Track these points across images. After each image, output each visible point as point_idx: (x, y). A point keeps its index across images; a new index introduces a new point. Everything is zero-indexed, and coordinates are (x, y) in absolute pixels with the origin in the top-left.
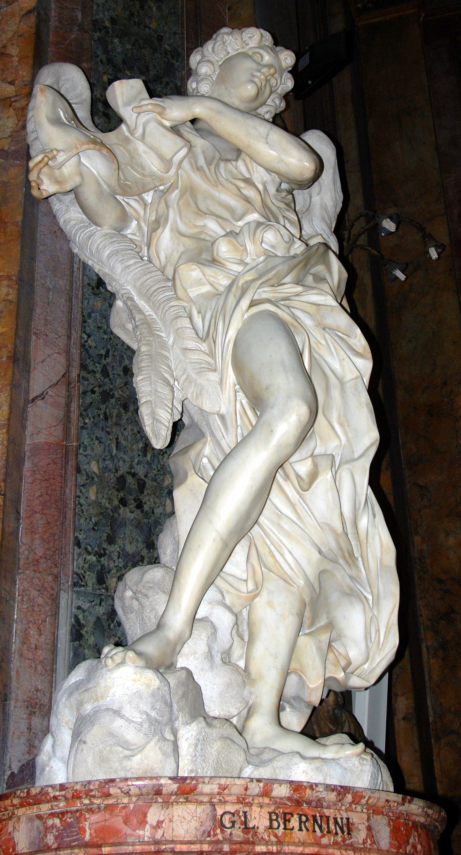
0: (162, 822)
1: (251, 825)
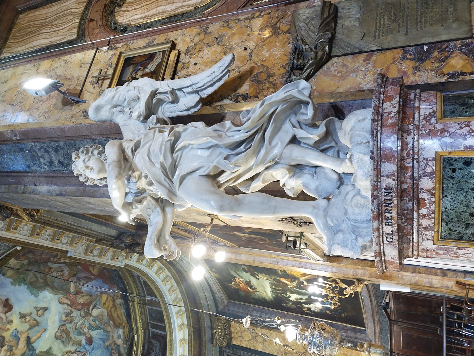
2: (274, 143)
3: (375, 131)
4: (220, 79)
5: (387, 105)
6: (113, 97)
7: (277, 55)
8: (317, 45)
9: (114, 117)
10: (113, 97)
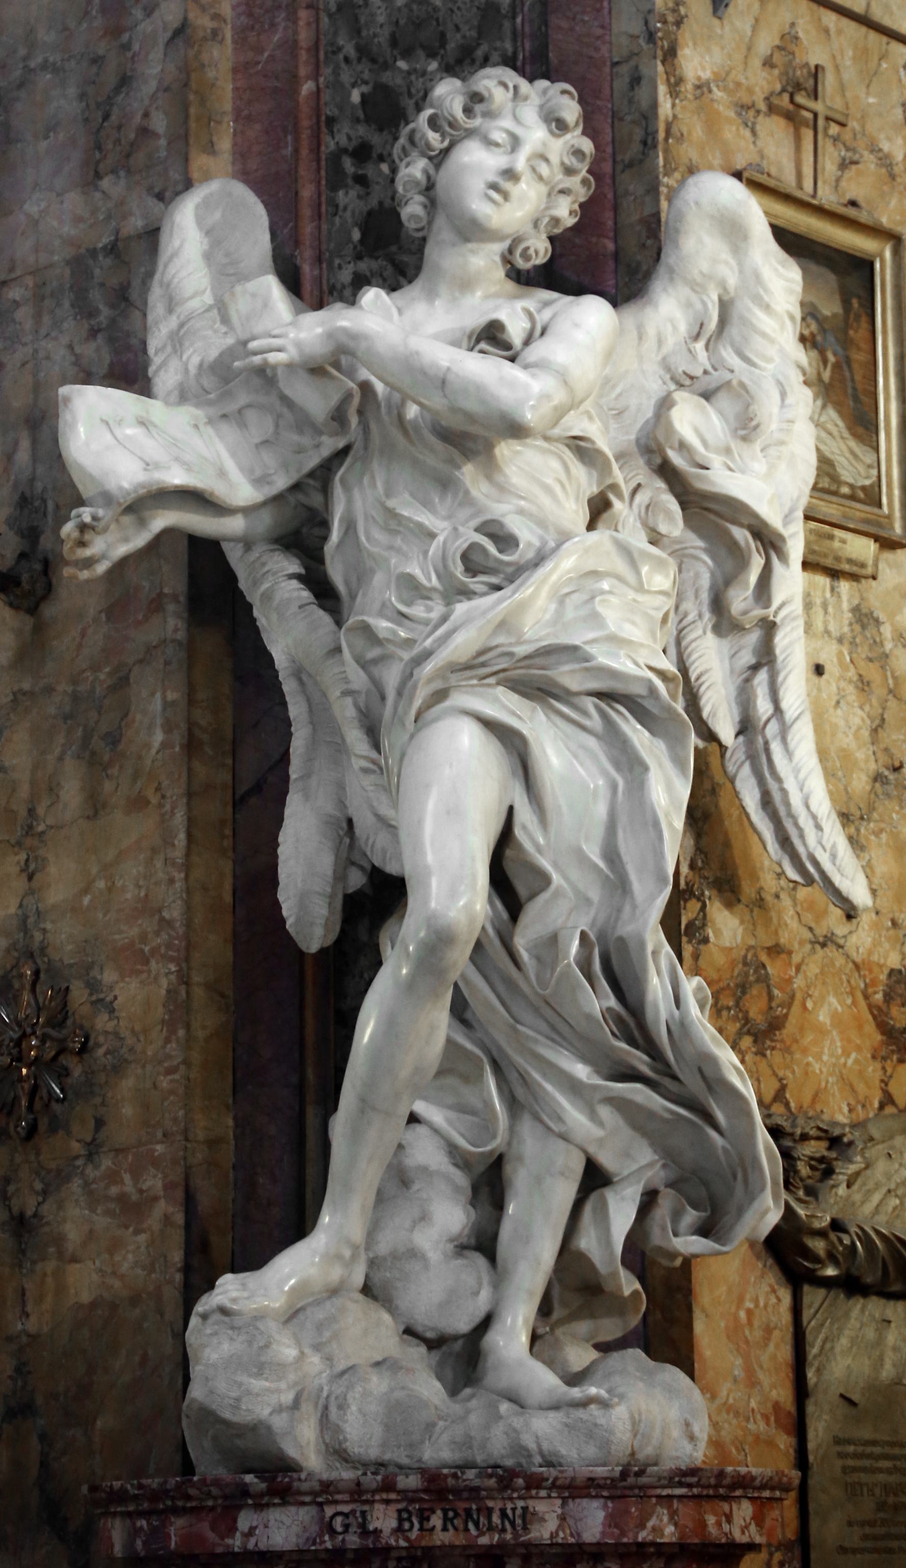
0: (256, 1527)
1: (371, 1528)
2: (605, 1112)
3: (695, 1480)
4: (785, 842)
5: (744, 1511)
6: (767, 308)
7: (818, 1057)
8: (846, 1231)
9: (684, 291)
10: (767, 308)
